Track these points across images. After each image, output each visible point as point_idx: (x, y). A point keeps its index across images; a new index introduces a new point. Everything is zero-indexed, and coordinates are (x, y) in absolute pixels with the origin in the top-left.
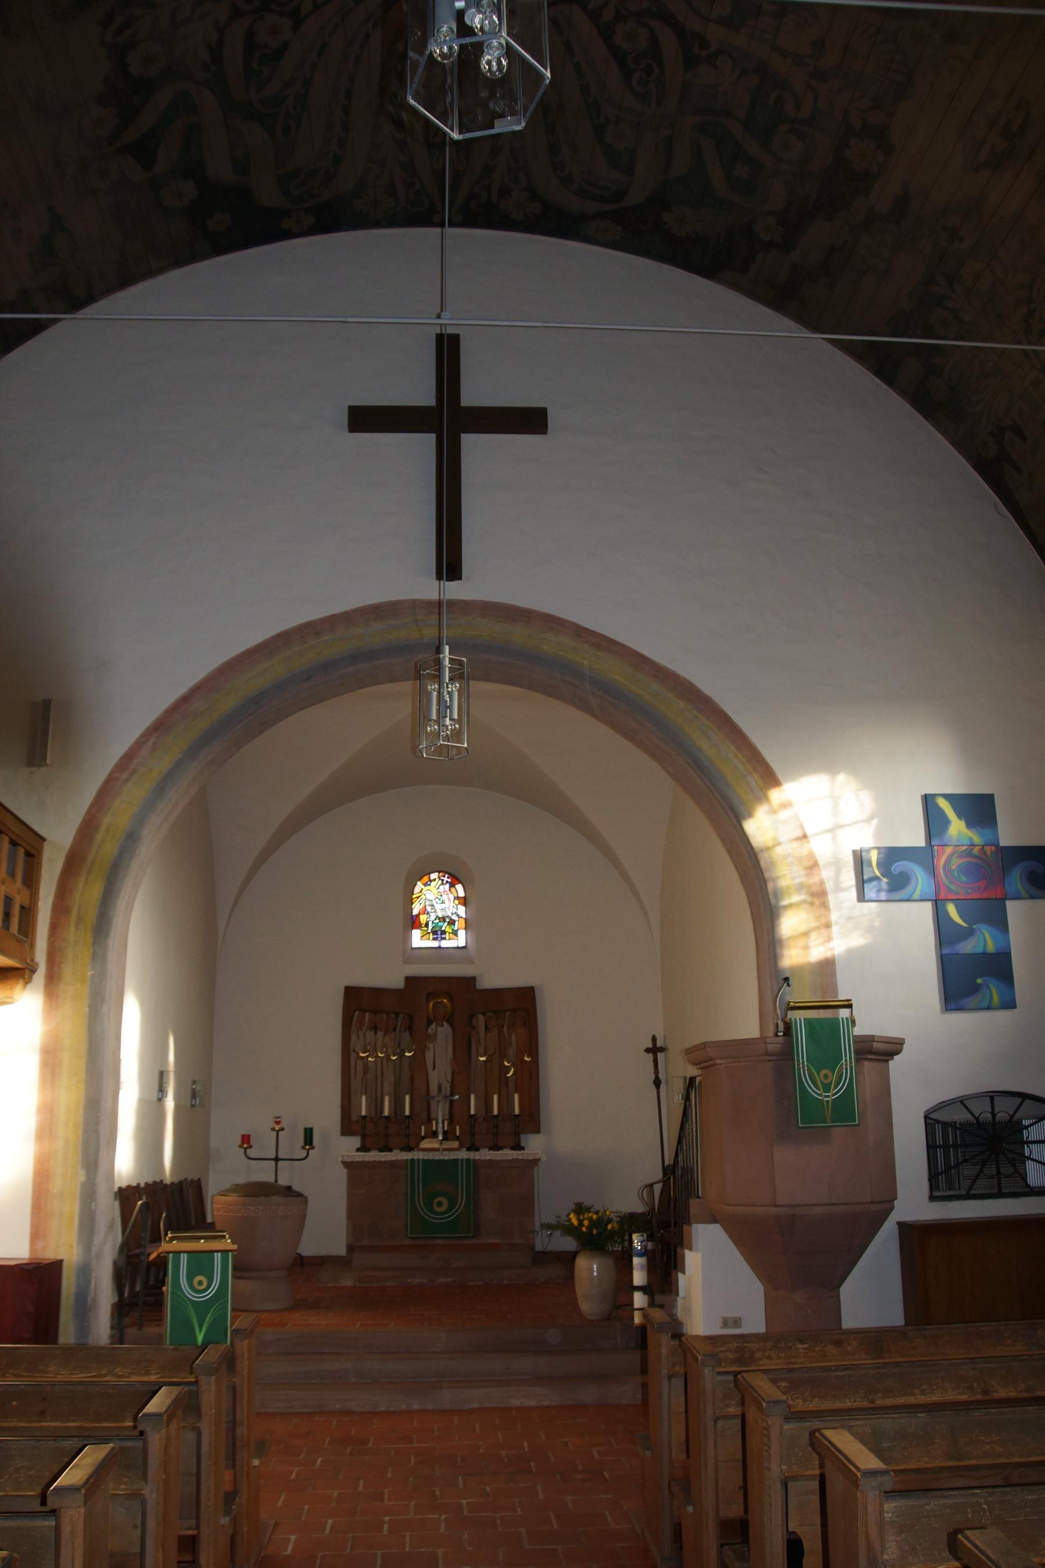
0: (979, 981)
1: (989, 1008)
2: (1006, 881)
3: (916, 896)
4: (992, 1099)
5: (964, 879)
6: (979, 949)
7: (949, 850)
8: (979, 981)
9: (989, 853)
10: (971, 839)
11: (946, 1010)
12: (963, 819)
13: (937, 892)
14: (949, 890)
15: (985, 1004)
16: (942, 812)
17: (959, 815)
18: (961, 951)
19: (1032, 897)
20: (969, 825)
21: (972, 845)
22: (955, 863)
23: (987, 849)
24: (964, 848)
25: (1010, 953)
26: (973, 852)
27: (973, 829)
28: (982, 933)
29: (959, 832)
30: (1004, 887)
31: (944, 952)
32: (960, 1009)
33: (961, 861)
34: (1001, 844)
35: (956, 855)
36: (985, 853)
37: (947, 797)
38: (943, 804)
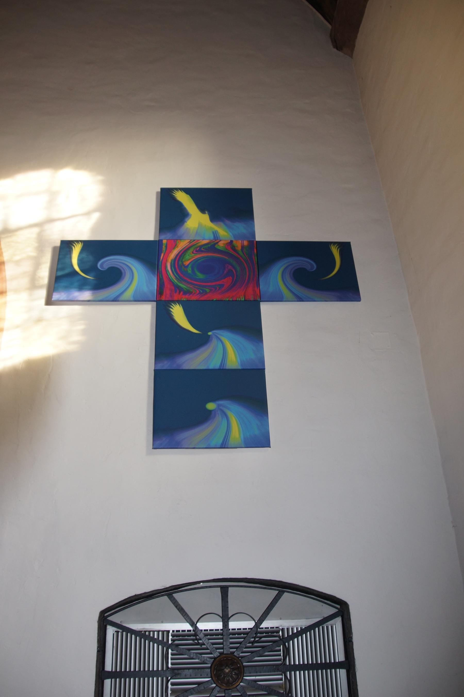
0: (211, 406)
1: (224, 445)
2: (261, 280)
3: (129, 293)
4: (224, 592)
5: (200, 276)
6: (215, 364)
7: (182, 245)
8: (211, 406)
9: (239, 248)
10: (215, 233)
11: (155, 447)
12: (206, 212)
13: (160, 292)
14: (179, 289)
15: (219, 439)
16: (180, 205)
17: (202, 209)
18: (186, 367)
19: (300, 299)
20: (213, 219)
21: (217, 239)
22: (189, 258)
23: (238, 244)
24: (205, 242)
25: (265, 369)
26: (216, 246)
27: (222, 224)
28: (222, 342)
29: (200, 225)
30: (258, 285)
31: (159, 367)
32: (176, 446)
33: (198, 256)
34: (259, 237)
35: (191, 250)
36: (234, 249)
37: (187, 191)
38: (182, 197)
